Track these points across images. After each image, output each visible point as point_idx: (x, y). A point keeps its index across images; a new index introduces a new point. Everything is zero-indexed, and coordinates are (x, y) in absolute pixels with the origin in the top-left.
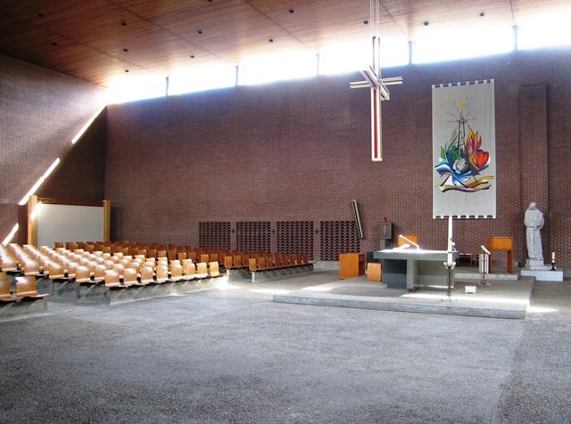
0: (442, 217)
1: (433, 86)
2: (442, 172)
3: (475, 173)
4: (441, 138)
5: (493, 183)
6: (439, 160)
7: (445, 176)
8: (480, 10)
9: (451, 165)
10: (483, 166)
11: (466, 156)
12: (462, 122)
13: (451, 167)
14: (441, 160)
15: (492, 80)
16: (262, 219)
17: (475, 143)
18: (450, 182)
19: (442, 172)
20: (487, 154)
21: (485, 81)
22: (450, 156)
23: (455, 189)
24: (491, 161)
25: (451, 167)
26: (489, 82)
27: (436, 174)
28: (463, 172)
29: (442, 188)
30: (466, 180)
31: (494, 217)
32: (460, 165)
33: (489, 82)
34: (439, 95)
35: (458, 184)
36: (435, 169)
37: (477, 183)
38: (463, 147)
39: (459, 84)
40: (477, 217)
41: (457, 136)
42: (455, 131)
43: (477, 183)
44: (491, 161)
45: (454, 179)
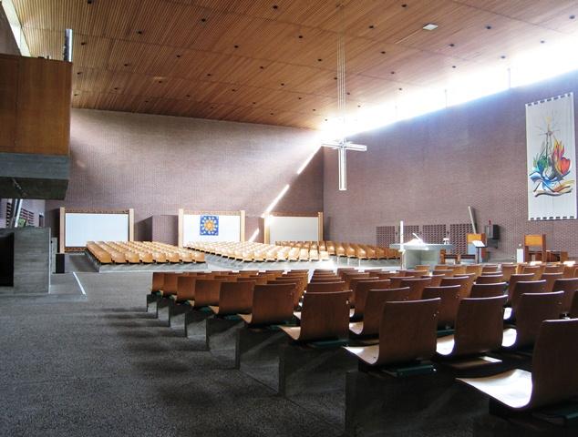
0: (561, 218)
1: (527, 105)
2: (535, 179)
3: (560, 179)
4: (533, 151)
5: (574, 186)
6: (532, 169)
7: (537, 183)
8: (448, 41)
9: (541, 172)
10: (566, 172)
11: (552, 164)
12: (549, 134)
13: (542, 174)
14: (534, 169)
15: (572, 94)
16: (414, 224)
17: (559, 152)
18: (541, 189)
19: (535, 179)
20: (568, 161)
21: (566, 95)
22: (541, 165)
23: (545, 194)
24: (572, 167)
25: (542, 174)
26: (569, 95)
27: (530, 181)
28: (551, 178)
29: (535, 194)
30: (554, 185)
31: (575, 218)
32: (548, 172)
33: (569, 95)
34: (532, 112)
35: (547, 189)
36: (529, 177)
37: (561, 188)
38: (550, 156)
39: (546, 100)
40: (568, 218)
41: (546, 146)
42: (544, 143)
43: (561, 188)
44: (572, 167)
45: (544, 185)
